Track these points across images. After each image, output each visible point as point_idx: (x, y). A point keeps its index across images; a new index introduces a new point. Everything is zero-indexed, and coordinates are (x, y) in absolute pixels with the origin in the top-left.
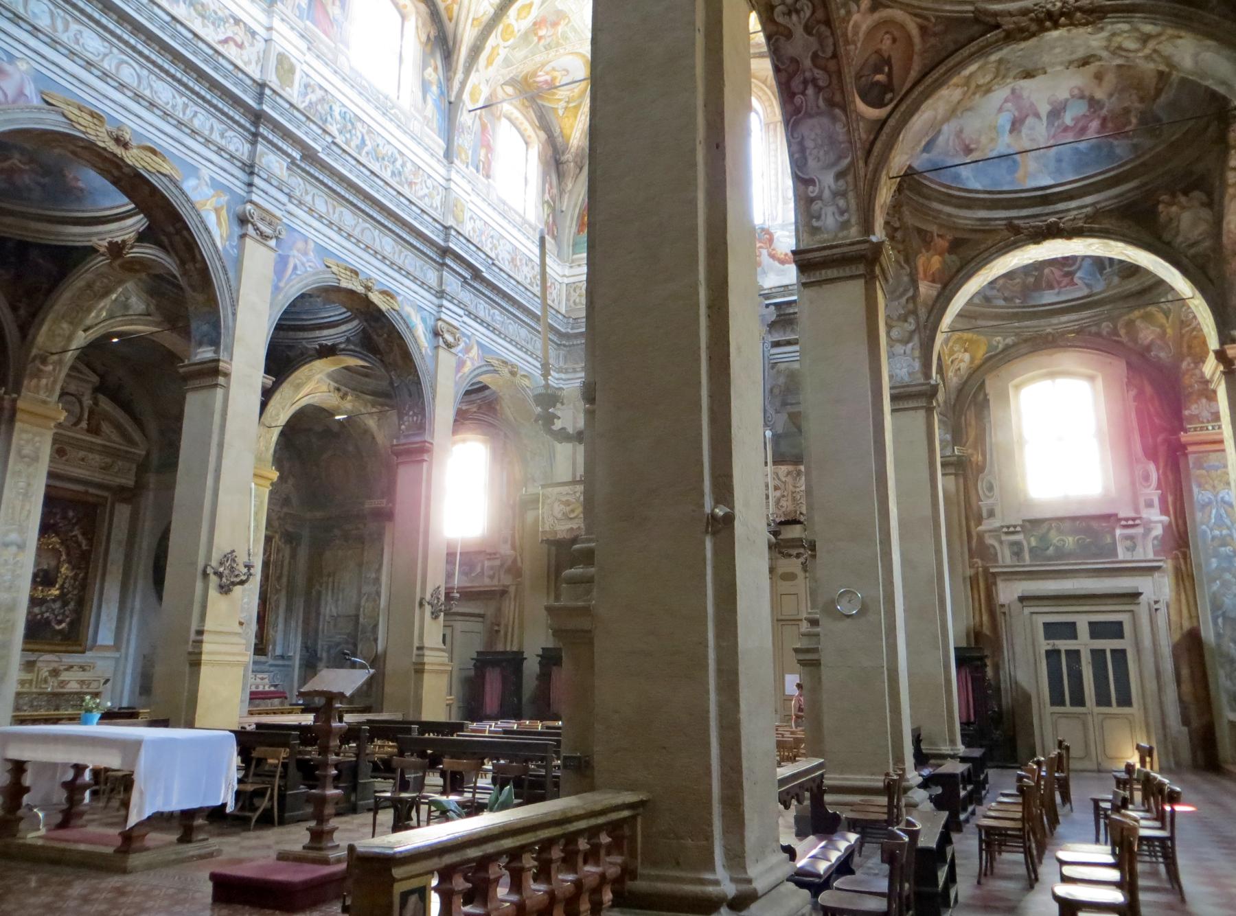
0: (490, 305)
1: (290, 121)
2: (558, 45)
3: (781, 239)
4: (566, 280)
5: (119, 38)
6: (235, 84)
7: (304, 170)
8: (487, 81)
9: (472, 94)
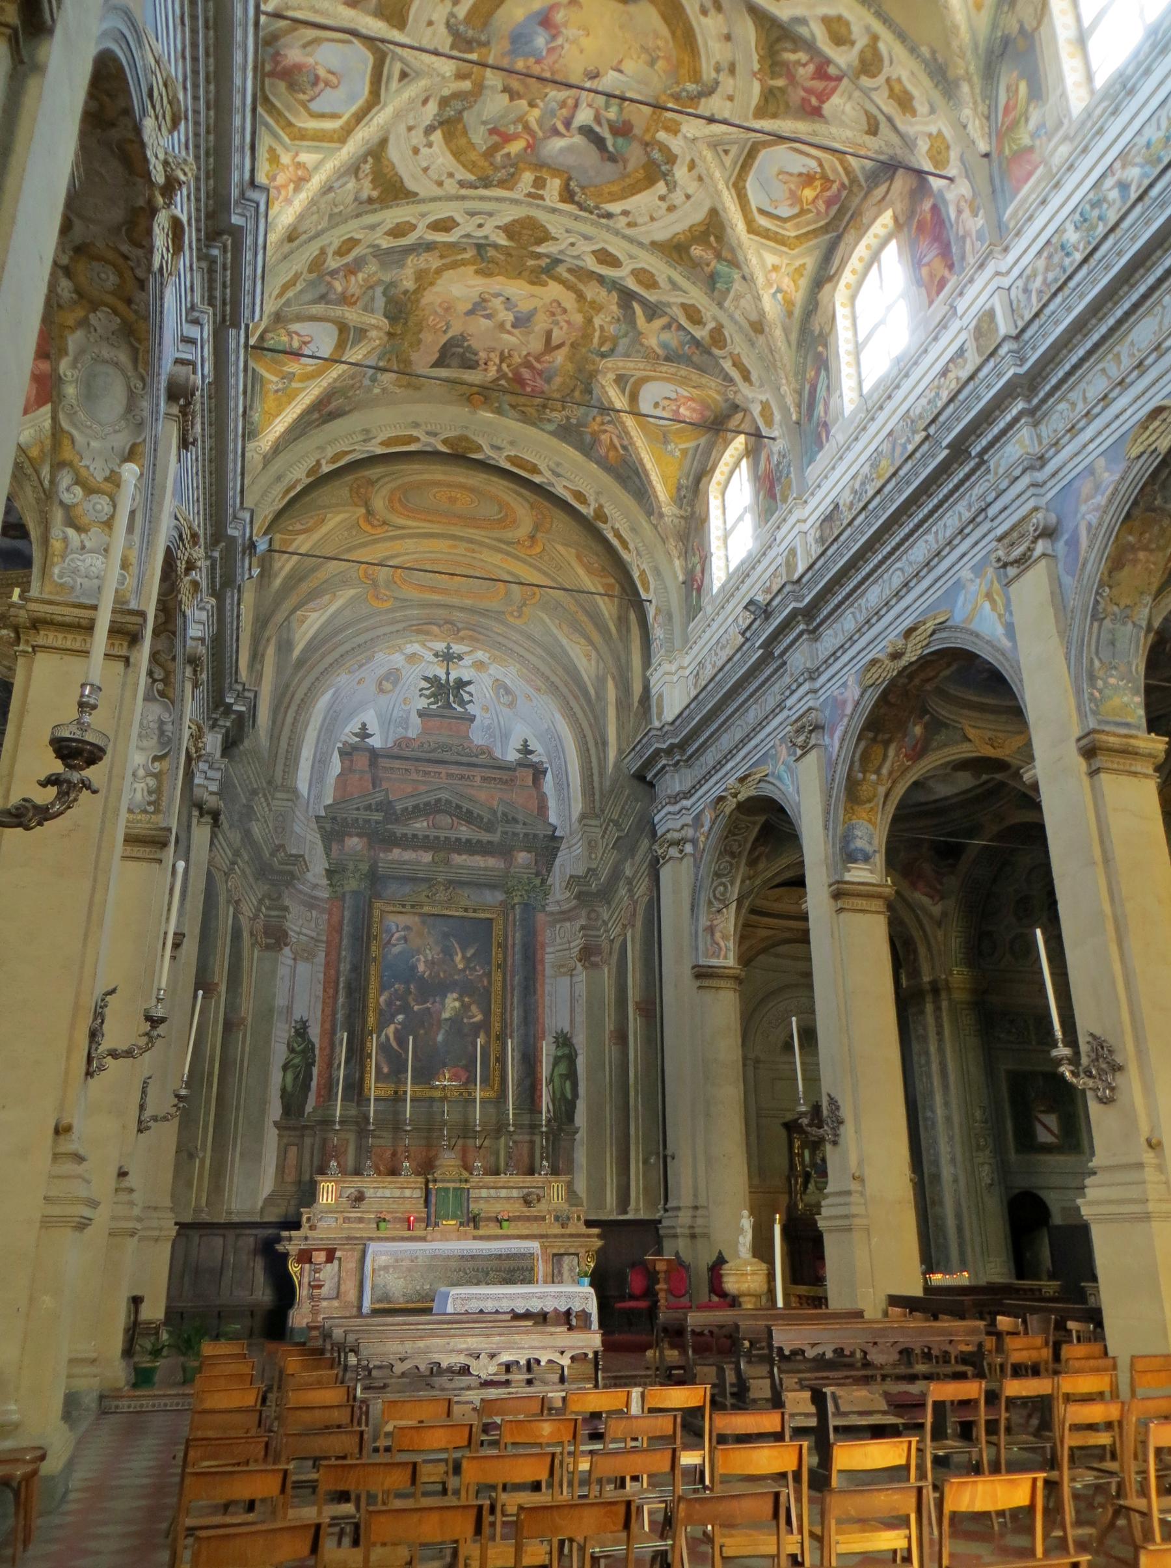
1: (969, 410)
5: (881, 563)
6: (925, 466)
7: (1050, 394)
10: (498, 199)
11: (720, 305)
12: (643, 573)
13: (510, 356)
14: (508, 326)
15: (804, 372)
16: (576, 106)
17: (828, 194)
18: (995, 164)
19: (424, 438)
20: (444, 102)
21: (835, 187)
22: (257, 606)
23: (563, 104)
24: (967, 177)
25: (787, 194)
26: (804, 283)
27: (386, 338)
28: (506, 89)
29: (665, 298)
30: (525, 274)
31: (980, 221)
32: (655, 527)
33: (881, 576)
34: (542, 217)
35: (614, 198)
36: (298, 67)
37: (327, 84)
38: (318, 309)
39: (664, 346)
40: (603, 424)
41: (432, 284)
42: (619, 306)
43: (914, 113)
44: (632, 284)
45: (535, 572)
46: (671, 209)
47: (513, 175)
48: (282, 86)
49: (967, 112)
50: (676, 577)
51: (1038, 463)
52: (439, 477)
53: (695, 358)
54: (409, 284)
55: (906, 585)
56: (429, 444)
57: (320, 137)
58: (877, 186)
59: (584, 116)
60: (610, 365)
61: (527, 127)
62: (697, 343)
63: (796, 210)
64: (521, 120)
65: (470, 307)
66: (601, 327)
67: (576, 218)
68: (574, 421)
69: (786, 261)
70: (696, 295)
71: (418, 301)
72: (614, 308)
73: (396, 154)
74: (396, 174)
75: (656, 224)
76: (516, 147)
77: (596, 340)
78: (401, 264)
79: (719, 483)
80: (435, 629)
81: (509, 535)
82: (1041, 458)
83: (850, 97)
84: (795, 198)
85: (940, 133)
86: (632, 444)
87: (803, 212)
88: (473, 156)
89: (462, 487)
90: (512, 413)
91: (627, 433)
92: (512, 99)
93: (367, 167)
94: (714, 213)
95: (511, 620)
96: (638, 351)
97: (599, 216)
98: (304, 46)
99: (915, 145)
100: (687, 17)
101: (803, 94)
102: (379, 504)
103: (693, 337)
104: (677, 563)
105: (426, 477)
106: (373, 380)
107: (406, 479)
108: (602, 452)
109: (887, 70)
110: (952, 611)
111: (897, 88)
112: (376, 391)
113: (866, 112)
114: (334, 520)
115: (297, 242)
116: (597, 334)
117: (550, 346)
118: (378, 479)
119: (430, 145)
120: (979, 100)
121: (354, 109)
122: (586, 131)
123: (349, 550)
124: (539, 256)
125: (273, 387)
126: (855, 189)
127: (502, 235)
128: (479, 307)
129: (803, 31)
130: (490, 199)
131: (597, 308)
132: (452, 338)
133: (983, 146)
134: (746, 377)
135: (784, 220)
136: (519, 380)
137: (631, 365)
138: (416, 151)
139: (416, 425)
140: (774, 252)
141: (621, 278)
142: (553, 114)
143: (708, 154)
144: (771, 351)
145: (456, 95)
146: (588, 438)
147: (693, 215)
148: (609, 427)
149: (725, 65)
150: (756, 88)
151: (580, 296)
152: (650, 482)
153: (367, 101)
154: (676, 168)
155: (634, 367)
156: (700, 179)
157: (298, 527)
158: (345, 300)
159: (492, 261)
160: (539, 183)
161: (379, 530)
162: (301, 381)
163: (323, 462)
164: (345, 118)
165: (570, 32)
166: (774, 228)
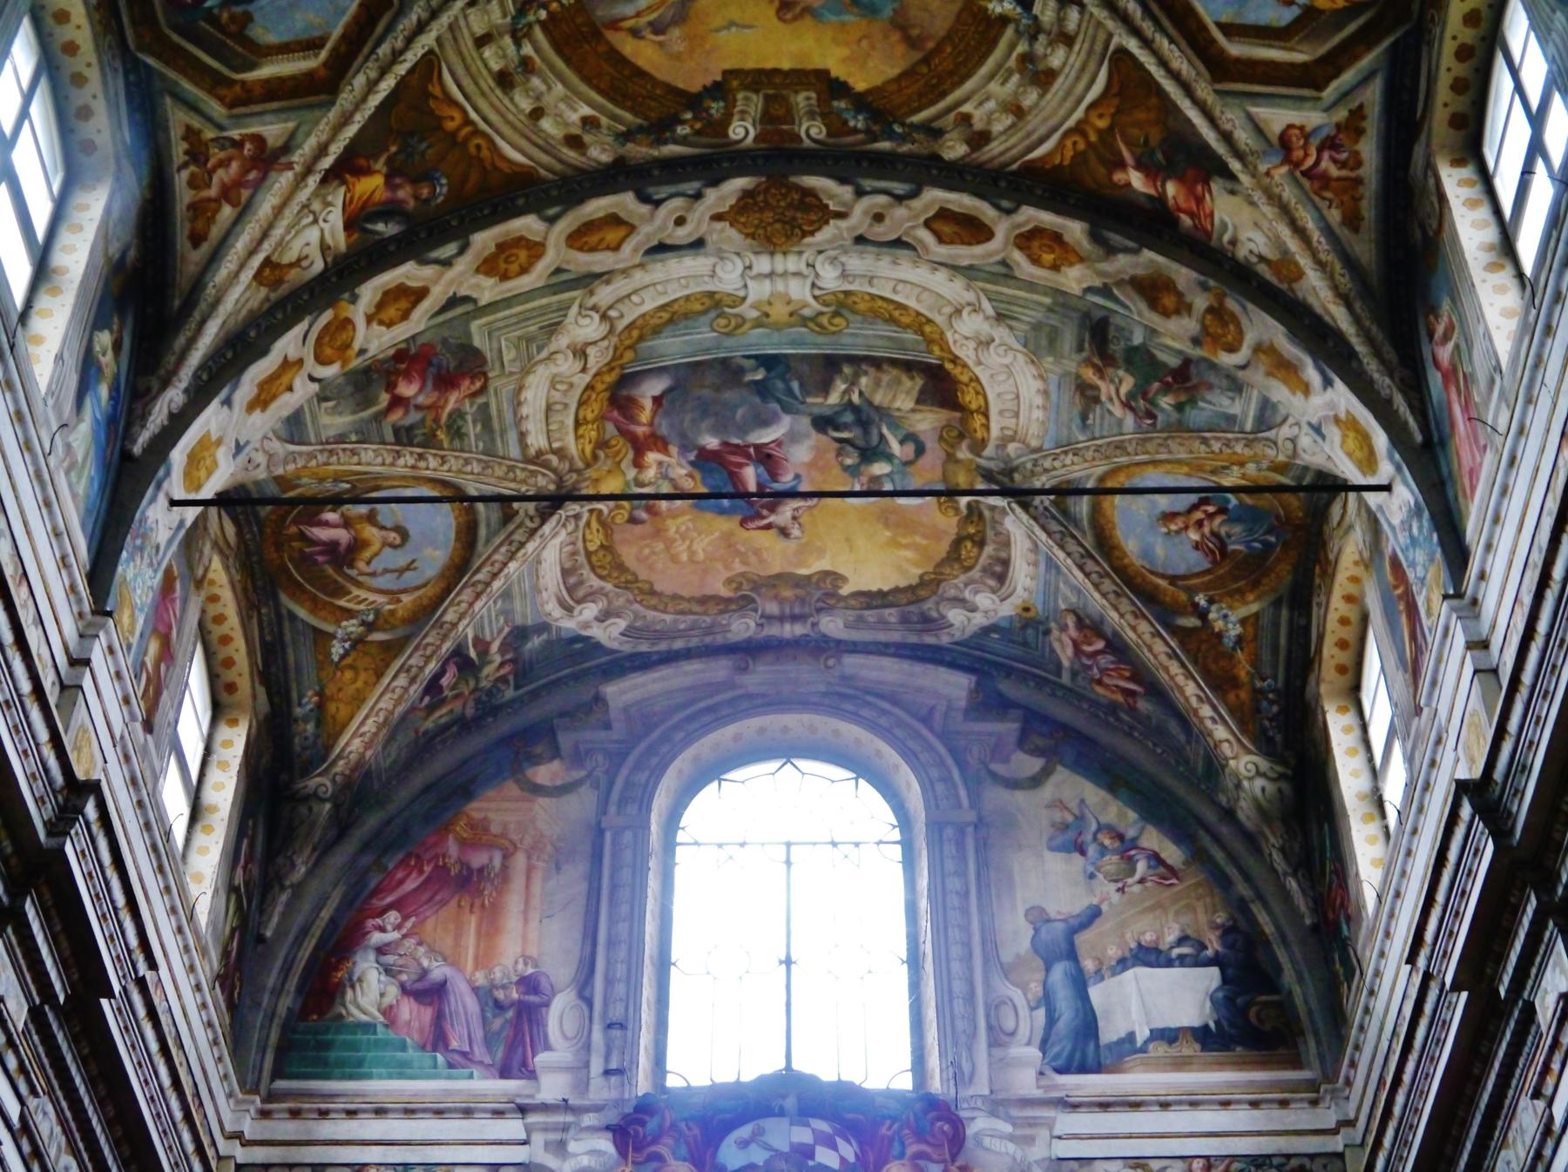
0: (66, 1131)
2: (430, 442)
3: (987, 1141)
4: (242, 1155)
8: (239, 448)
9: (194, 459)
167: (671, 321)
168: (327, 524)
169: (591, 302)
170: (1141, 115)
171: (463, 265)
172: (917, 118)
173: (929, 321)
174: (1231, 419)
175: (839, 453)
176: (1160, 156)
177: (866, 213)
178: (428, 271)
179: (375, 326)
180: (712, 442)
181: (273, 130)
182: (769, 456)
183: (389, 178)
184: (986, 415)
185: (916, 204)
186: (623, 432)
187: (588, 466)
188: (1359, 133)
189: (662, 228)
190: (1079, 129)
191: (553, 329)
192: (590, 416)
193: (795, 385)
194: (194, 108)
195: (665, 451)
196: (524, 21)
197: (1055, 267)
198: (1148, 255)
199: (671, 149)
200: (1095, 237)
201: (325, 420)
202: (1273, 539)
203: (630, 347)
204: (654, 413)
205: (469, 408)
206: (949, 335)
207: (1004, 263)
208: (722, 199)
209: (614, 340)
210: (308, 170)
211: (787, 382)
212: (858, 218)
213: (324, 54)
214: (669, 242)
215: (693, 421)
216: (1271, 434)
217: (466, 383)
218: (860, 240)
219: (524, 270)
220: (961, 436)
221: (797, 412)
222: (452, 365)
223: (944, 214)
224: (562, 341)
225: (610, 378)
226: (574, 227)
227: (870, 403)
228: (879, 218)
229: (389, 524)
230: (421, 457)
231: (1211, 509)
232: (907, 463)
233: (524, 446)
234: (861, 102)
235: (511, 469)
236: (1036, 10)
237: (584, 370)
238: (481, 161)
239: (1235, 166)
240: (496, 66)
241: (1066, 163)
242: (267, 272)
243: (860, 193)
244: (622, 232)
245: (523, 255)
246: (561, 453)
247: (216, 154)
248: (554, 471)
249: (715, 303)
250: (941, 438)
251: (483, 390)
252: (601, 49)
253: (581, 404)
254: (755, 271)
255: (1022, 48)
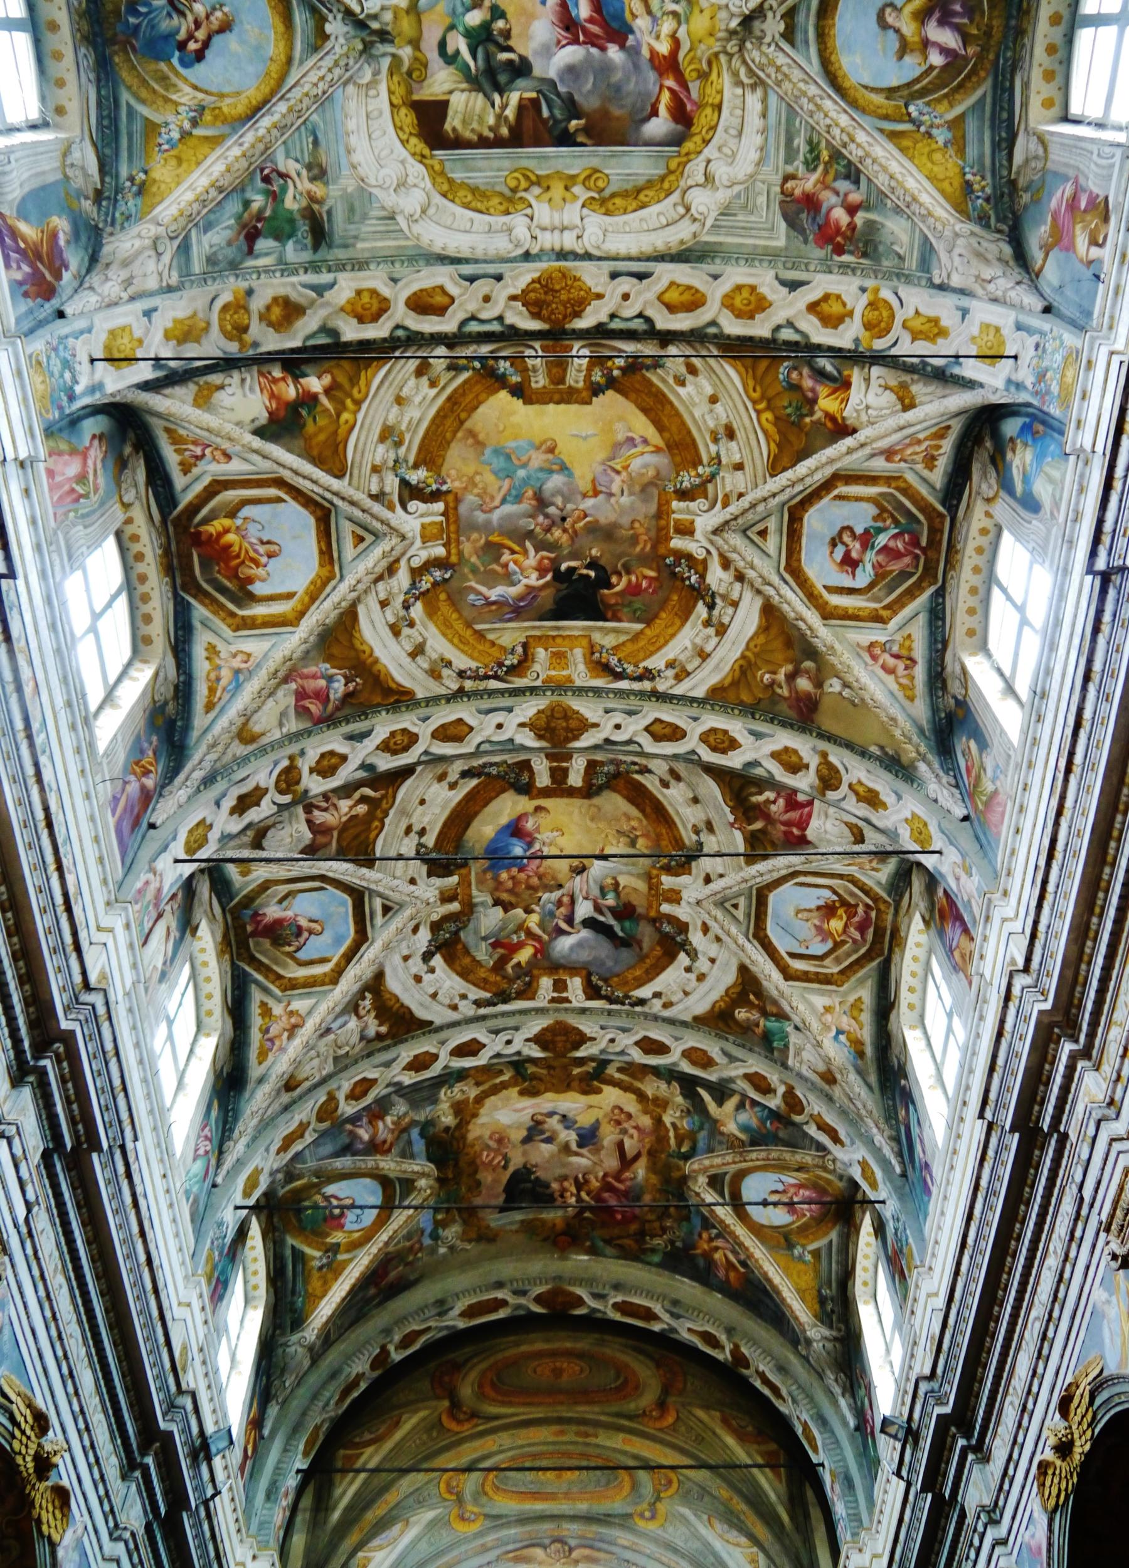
2: (836, 155)
7: (1094, 1024)
10: (523, 1012)
11: (784, 1065)
12: (805, 1425)
13: (587, 1181)
14: (574, 1147)
15: (896, 1114)
16: (573, 902)
17: (856, 919)
18: (976, 823)
19: (512, 1300)
20: (435, 927)
21: (861, 910)
22: (308, 1550)
23: (559, 903)
24: (951, 843)
25: (814, 931)
26: (866, 1017)
27: (436, 1185)
28: (497, 902)
29: (726, 1074)
30: (575, 1084)
31: (976, 878)
32: (806, 1359)
33: (1021, 1337)
34: (574, 1021)
35: (641, 983)
36: (279, 922)
37: (311, 932)
38: (344, 1163)
39: (745, 1128)
40: (711, 1240)
41: (475, 1115)
42: (685, 1096)
43: (884, 806)
44: (686, 1067)
45: (668, 1451)
46: (701, 978)
47: (529, 984)
48: (266, 943)
49: (933, 788)
50: (845, 1424)
51: (1111, 1112)
52: (540, 1346)
53: (781, 1134)
54: (448, 1120)
55: (1044, 1337)
56: (519, 1307)
57: (311, 983)
58: (902, 896)
59: (584, 910)
60: (696, 1166)
61: (529, 934)
62: (774, 1115)
63: (830, 944)
64: (521, 927)
65: (524, 1133)
66: (673, 1124)
67: (610, 1013)
68: (679, 1244)
69: (837, 1000)
70: (755, 1064)
71: (464, 1137)
72: (679, 1099)
73: (397, 984)
74: (402, 1005)
75: (691, 999)
76: (524, 955)
77: (672, 1141)
78: (435, 1101)
79: (865, 1284)
80: (538, 1552)
81: (632, 1406)
82: (1111, 1103)
83: (826, 816)
84: (824, 934)
85: (914, 815)
86: (750, 1256)
87: (837, 945)
88: (482, 973)
89: (569, 1354)
90: (609, 1250)
91: (741, 1245)
92: (506, 911)
93: (367, 1003)
94: (743, 969)
95: (641, 1524)
96: (720, 1143)
97: (632, 1005)
98: (280, 902)
99: (898, 835)
100: (650, 793)
101: (783, 828)
102: (466, 1391)
103: (770, 1110)
104: (842, 1402)
105: (524, 1348)
106: (435, 1237)
107: (499, 1356)
108: (721, 1274)
109: (846, 779)
110: (1102, 1358)
111: (861, 790)
112: (442, 1250)
113: (846, 824)
114: (410, 1423)
115: (299, 1091)
116: (672, 1134)
117: (626, 1162)
118: (467, 1360)
119: (432, 970)
120: (941, 773)
121: (342, 950)
122: (589, 923)
123: (427, 1458)
124: (581, 1061)
125: (316, 1264)
126: (882, 907)
127: (534, 1046)
128: (535, 1131)
129: (759, 771)
130: (513, 1013)
131: (662, 1104)
132: (516, 1173)
133: (960, 812)
134: (836, 1139)
135: (821, 958)
136: (603, 1210)
137: (718, 1161)
138: (418, 979)
139: (499, 1285)
140: (823, 993)
141: (675, 1064)
142: (552, 914)
143: (719, 914)
144: (851, 1100)
145: (446, 918)
146: (701, 1262)
147: (723, 979)
148: (719, 1243)
149: (702, 826)
150: (738, 836)
151: (641, 1096)
152: (783, 1300)
153: (354, 940)
154: (691, 936)
155: (723, 1161)
156: (718, 939)
157: (367, 1436)
158: (375, 1147)
159: (534, 1077)
160: (560, 986)
161: (467, 1426)
162: (348, 1251)
163: (391, 1348)
164: (335, 960)
165: (544, 836)
166: (813, 969)
167: (639, 191)
168: (944, 51)
169: (696, 227)
170: (322, 437)
171: (778, 316)
172: (465, 375)
173: (444, 195)
174: (208, 227)
175: (507, 34)
176: (304, 413)
177: (496, 302)
178: (803, 325)
179: (849, 307)
180: (614, 53)
181: (879, 465)
182: (567, 29)
183: (814, 401)
184: (392, 104)
185: (462, 316)
186: (683, 84)
187: (716, 55)
188: (181, 464)
189: (639, 293)
190: (358, 403)
191: (726, 212)
192: (708, 111)
193: (545, 113)
194: (924, 480)
195: (653, 52)
196: (712, 469)
197: (359, 293)
198: (297, 343)
199: (630, 347)
200: (334, 333)
201: (905, 238)
202: (132, 20)
203: (671, 172)
204: (658, 100)
205: (798, 167)
206: (429, 185)
207: (395, 281)
208: (596, 311)
209: (682, 183)
210: (862, 445)
211: (552, 115)
212: (501, 293)
213: (835, 492)
214: (635, 281)
215: (628, 80)
216: (176, 243)
217: (798, 192)
218: (499, 278)
219: (739, 288)
220: (409, 73)
221: (543, 80)
222: (804, 216)
223: (441, 311)
224: (722, 196)
225: (688, 146)
226: (700, 310)
227: (486, 95)
228: (487, 299)
229: (891, 32)
230: (845, 145)
231: (192, 46)
232: (452, 27)
233: (764, 101)
234: (501, 381)
235: (779, 83)
236: (397, 480)
237: (709, 161)
238: (754, 378)
239: (257, 442)
240: (733, 444)
241: (363, 373)
242: (907, 401)
243: (500, 319)
244: (667, 297)
245: (738, 302)
246: (739, 83)
247: (919, 458)
248: (744, 62)
249: (604, 203)
250: (426, 66)
251: (787, 178)
252: (667, 435)
253: (714, 128)
254: (574, 234)
255: (402, 451)
